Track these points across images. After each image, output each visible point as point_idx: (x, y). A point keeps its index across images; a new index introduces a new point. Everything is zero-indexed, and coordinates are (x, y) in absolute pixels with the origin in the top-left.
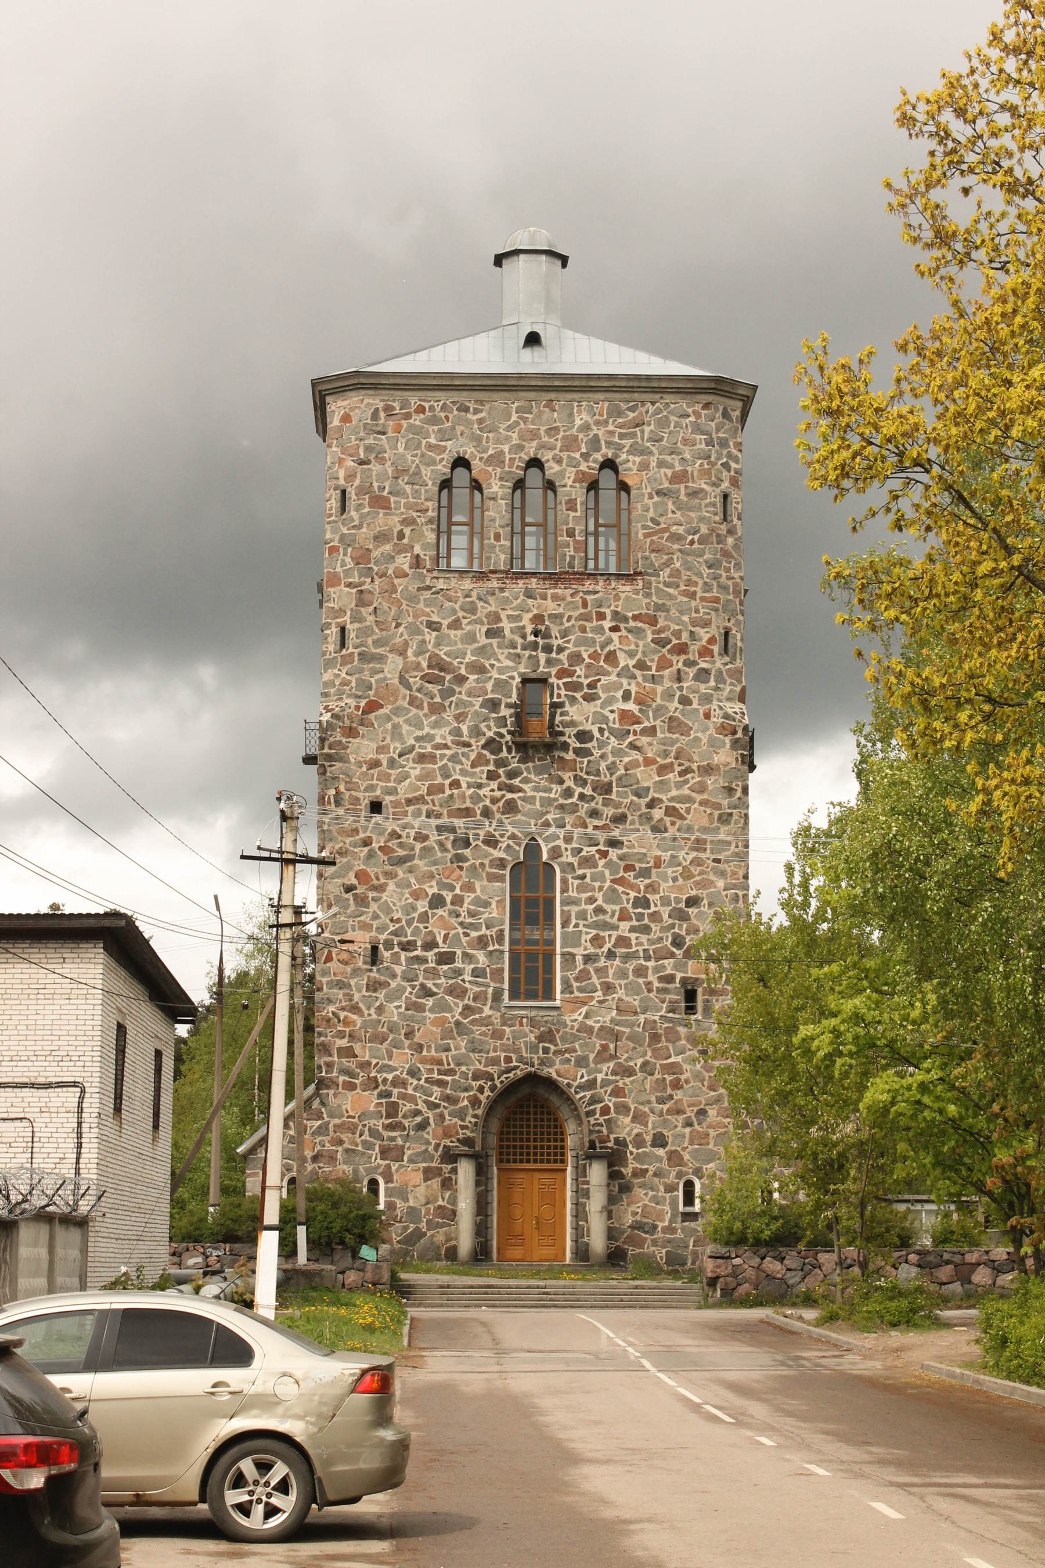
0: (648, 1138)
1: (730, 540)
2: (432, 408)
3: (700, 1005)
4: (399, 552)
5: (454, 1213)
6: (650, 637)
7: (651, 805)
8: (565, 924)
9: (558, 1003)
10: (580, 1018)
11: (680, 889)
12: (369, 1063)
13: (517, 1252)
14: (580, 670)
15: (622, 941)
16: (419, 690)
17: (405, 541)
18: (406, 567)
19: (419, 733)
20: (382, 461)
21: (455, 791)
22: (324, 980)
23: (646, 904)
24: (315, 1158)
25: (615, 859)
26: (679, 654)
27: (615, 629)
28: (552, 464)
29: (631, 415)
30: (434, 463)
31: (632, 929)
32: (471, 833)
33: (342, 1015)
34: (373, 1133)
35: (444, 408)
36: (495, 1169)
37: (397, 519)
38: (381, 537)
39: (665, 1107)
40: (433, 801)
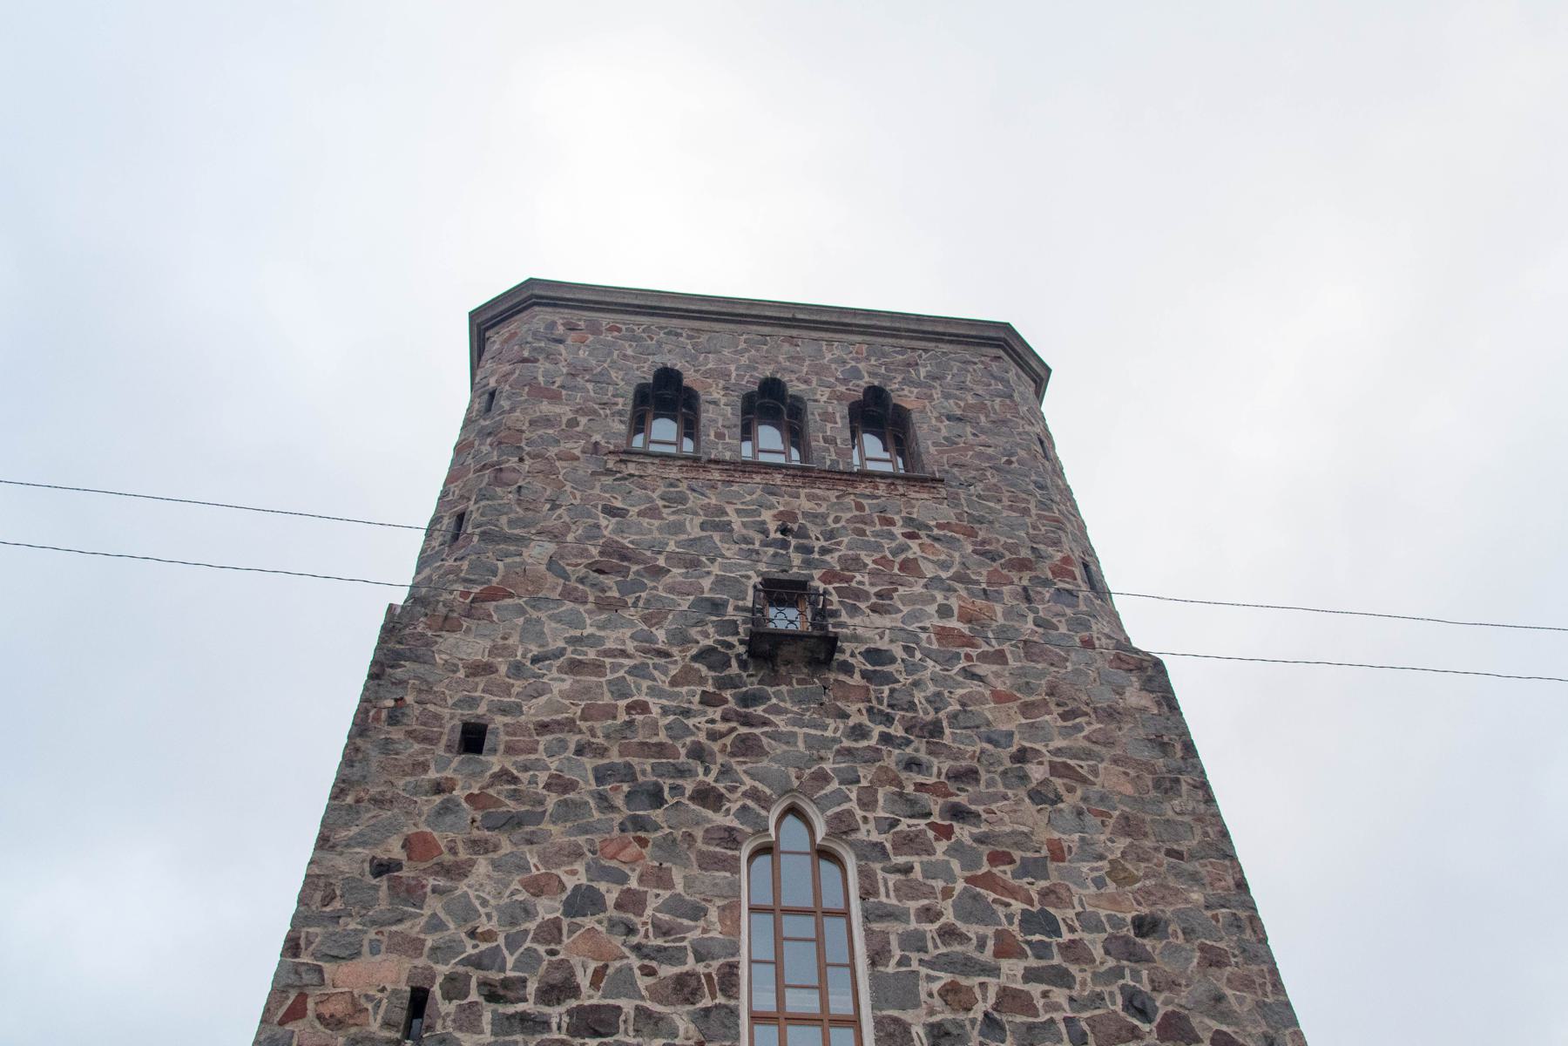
6: (970, 548)
7: (1022, 756)
15: (1009, 999)
19: (577, 633)
21: (639, 718)
25: (967, 840)
26: (1020, 570)
31: (1030, 975)
32: (666, 784)
40: (592, 731)
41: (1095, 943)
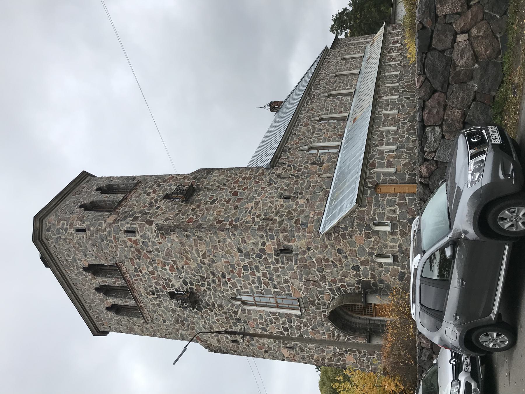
0: (355, 272)
11: (236, 255)
14: (161, 283)
25: (230, 276)
27: (141, 272)
31: (258, 271)
36: (376, 318)
39: (338, 265)
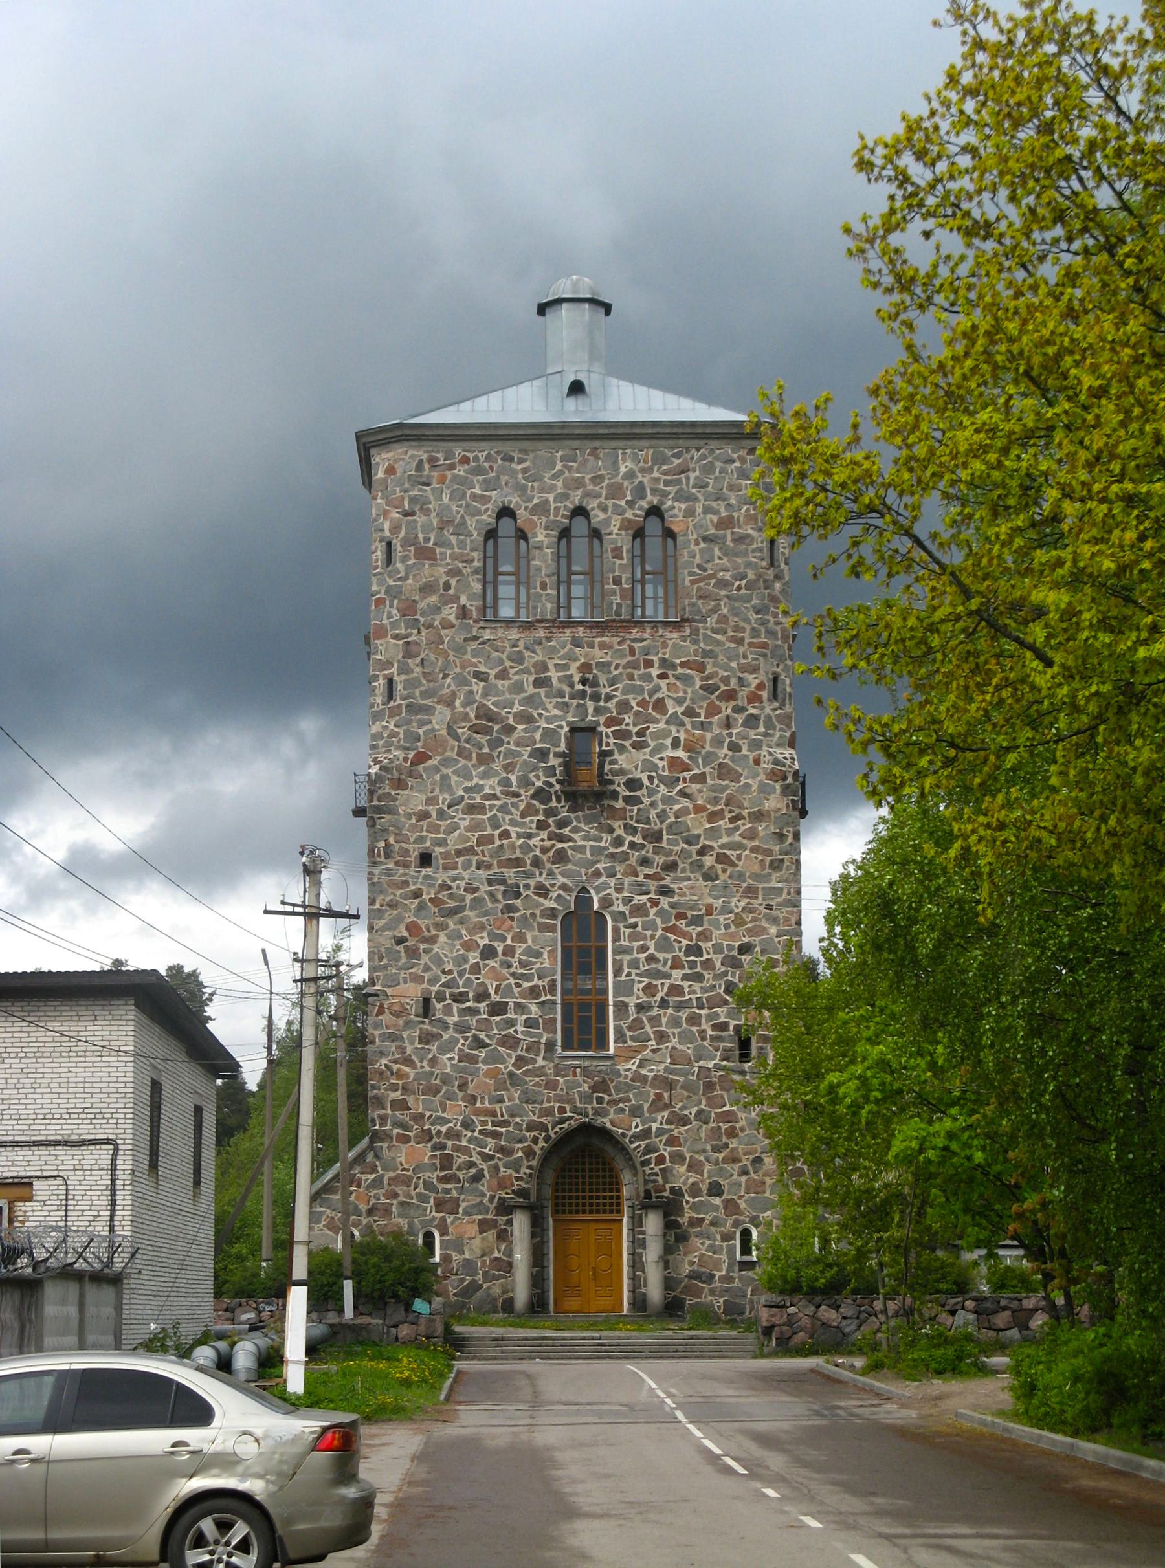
0: (704, 1187)
1: (778, 585)
2: (476, 459)
3: (754, 1052)
4: (446, 603)
5: (510, 1265)
6: (698, 684)
7: (702, 852)
8: (617, 973)
9: (611, 1051)
10: (634, 1068)
11: (733, 937)
12: (422, 1116)
13: (574, 1303)
14: (628, 719)
16: (467, 741)
17: (451, 592)
18: (452, 618)
19: (468, 784)
20: (426, 512)
22: (377, 1033)
23: (698, 951)
24: (370, 1212)
25: (666, 907)
27: (662, 676)
28: (597, 512)
29: (677, 461)
30: (479, 513)
31: (685, 978)
32: (522, 883)
33: (395, 1067)
34: (428, 1185)
35: (488, 458)
37: (442, 570)
38: (427, 589)
39: (721, 1156)
41: (718, 960)
